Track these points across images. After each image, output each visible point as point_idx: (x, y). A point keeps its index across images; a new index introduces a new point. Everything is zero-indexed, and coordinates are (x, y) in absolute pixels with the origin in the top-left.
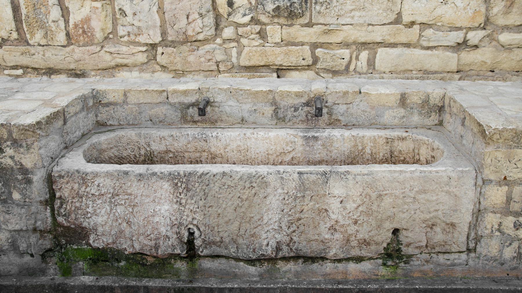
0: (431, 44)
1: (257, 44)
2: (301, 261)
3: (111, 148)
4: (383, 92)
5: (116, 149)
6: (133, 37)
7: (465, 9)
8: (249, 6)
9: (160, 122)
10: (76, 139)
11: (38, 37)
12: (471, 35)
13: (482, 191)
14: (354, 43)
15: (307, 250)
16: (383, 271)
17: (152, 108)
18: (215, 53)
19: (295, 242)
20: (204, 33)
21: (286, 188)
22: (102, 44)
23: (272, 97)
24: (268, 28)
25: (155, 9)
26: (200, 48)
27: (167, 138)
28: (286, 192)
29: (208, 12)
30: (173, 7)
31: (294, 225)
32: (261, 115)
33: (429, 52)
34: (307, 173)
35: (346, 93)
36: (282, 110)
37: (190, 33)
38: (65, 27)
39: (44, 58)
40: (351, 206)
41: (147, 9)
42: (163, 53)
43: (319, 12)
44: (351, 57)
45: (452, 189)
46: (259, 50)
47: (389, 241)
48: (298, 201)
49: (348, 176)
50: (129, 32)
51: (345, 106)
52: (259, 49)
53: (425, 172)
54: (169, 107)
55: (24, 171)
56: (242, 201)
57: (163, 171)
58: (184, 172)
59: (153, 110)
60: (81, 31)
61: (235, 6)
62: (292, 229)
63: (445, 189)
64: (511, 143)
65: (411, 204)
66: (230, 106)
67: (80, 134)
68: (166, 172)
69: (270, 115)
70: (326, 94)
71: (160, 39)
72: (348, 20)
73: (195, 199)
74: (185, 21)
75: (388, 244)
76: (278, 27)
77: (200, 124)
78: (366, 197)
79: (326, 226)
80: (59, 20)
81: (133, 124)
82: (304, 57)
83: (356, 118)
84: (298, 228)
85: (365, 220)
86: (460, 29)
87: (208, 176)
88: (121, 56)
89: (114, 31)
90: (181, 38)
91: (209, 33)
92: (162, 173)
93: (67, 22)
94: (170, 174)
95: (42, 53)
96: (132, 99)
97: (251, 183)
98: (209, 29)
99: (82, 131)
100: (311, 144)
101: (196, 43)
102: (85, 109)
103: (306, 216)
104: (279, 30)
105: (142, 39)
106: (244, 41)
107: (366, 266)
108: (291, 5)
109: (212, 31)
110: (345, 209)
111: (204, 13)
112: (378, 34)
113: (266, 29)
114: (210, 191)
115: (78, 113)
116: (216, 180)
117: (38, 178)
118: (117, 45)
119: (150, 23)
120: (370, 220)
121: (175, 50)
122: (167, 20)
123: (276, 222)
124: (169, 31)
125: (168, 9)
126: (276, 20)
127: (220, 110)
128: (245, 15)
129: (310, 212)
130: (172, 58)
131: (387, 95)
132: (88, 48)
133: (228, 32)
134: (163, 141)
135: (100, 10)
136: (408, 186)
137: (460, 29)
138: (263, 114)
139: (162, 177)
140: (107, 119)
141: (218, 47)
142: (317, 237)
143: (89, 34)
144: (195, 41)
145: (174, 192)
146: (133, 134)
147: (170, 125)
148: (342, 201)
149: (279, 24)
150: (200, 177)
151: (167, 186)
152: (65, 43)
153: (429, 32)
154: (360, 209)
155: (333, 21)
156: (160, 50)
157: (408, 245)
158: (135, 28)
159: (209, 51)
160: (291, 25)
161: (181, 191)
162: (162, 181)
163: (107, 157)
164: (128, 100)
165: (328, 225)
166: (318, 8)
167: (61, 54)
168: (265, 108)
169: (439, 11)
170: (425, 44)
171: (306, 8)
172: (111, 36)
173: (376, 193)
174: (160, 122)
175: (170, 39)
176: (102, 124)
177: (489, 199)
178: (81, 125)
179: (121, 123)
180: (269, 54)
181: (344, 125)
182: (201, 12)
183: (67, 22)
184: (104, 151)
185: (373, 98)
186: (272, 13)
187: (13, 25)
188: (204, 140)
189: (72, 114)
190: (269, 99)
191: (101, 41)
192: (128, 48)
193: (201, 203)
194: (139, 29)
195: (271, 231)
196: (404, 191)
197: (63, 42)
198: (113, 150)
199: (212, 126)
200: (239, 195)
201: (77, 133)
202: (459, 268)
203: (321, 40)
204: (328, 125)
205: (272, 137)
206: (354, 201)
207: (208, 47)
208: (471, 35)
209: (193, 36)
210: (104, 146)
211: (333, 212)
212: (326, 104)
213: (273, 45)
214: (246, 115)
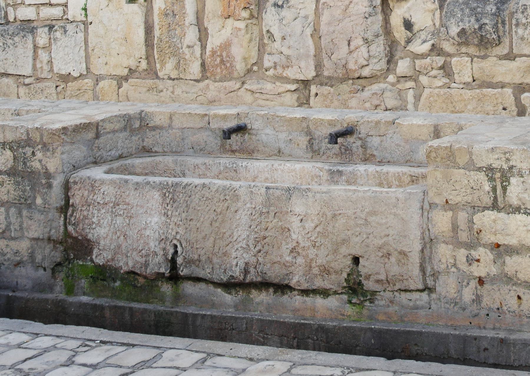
1: (440, 84)
2: (271, 290)
4: (415, 123)
6: (280, 70)
8: (432, 29)
9: (201, 150)
11: (168, 68)
13: (430, 216)
15: (274, 274)
16: (349, 310)
17: (195, 134)
18: (384, 96)
19: (260, 264)
20: (370, 67)
21: (254, 203)
22: (243, 79)
23: (306, 125)
24: (454, 60)
25: (309, 31)
26: (366, 89)
27: (200, 166)
28: (254, 207)
29: (377, 36)
30: (332, 29)
31: (259, 244)
32: (296, 146)
34: (274, 189)
35: (378, 123)
36: (317, 141)
37: (352, 66)
38: (201, 54)
39: (173, 96)
40: (309, 225)
41: (299, 32)
42: (317, 94)
43: (522, 39)
45: (399, 211)
46: (442, 93)
47: (348, 270)
48: (263, 217)
49: (309, 194)
50: (275, 63)
51: (378, 138)
52: (442, 91)
53: (376, 192)
54: (210, 133)
56: (217, 215)
57: (155, 180)
58: (173, 181)
59: (195, 137)
60: (218, 60)
61: (416, 28)
62: (257, 248)
63: (393, 211)
64: (449, 162)
65: (363, 227)
66: (265, 134)
68: (158, 182)
69: (304, 147)
70: (359, 123)
71: (314, 74)
73: (179, 211)
74: (345, 49)
75: (349, 275)
76: (467, 59)
77: (237, 154)
78: (322, 217)
79: (288, 247)
80: (195, 44)
81: (176, 152)
82: (505, 106)
83: (391, 153)
84: (263, 247)
85: (322, 242)
87: (190, 187)
88: (264, 97)
89: (259, 62)
90: (340, 72)
91: (378, 67)
92: (154, 182)
93: (203, 47)
94: (161, 183)
95: (171, 89)
96: (177, 123)
97: (225, 195)
98: (376, 60)
100: (335, 179)
101: (360, 81)
102: (128, 130)
103: (270, 234)
104: (469, 64)
105: (291, 73)
106: (424, 80)
107: (333, 302)
108: (480, 28)
109: (383, 64)
110: (304, 229)
111: (370, 38)
113: (451, 62)
114: (191, 202)
116: (196, 191)
118: (261, 81)
119: (301, 51)
120: (326, 243)
121: (332, 90)
122: (323, 47)
123: (244, 239)
124: (326, 62)
125: (325, 32)
126: (464, 49)
127: (257, 138)
128: (424, 42)
129: (274, 229)
130: (329, 101)
131: (419, 126)
132: (225, 84)
133: (403, 66)
134: (197, 170)
135: (243, 32)
136: (360, 206)
138: (298, 145)
139: (153, 186)
140: (152, 144)
141: (390, 87)
142: (279, 259)
143: (228, 65)
144: (359, 78)
145: (163, 203)
146: (171, 161)
148: (302, 220)
149: (468, 55)
150: (184, 188)
151: (157, 195)
152: (198, 76)
154: (318, 229)
156: (314, 89)
157: (368, 277)
158: (283, 58)
159: (376, 93)
161: (168, 202)
162: (154, 190)
164: (173, 124)
165: (290, 246)
166: (520, 31)
167: (193, 91)
168: (300, 138)
171: (504, 32)
172: (255, 68)
173: (331, 212)
174: (201, 150)
175: (326, 73)
176: (148, 150)
177: (437, 226)
179: (165, 150)
180: (456, 100)
181: (379, 162)
182: (366, 36)
183: (203, 47)
185: (405, 129)
186: (457, 38)
188: (235, 171)
190: (303, 128)
191: (242, 75)
192: (274, 85)
193: (184, 215)
194: (288, 59)
195: (240, 249)
196: (356, 211)
197: (196, 75)
199: (249, 157)
200: (214, 208)
202: (422, 312)
204: (363, 161)
205: (298, 169)
206: (312, 220)
207: (376, 87)
209: (356, 70)
211: (294, 232)
212: (359, 136)
213: (461, 86)
214: (282, 146)
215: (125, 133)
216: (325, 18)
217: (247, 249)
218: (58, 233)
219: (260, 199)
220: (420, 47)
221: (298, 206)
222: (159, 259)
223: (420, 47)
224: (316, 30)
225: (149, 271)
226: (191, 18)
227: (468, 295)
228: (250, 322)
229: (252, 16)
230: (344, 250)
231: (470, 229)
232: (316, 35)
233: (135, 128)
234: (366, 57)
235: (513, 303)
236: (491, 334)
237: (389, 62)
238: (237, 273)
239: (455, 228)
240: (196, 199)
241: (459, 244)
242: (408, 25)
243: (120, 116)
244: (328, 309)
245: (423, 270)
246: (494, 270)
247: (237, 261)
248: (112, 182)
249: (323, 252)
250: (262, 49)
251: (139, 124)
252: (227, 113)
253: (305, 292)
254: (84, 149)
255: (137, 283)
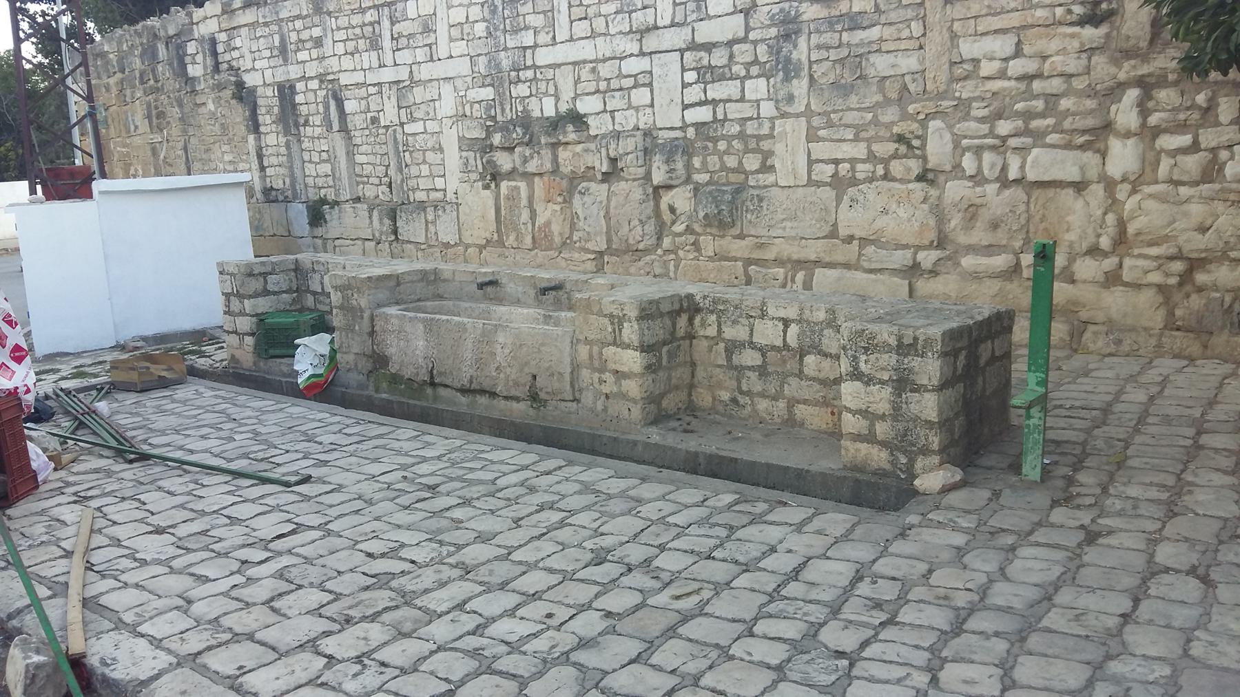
0: (873, 266)
7: (909, 220)
11: (511, 240)
12: (921, 256)
14: (789, 260)
15: (487, 385)
16: (532, 412)
25: (602, 213)
29: (649, 218)
33: (873, 276)
37: (631, 241)
40: (507, 351)
44: (786, 278)
55: (362, 311)
61: (678, 212)
66: (511, 288)
72: (779, 232)
86: (906, 247)
90: (623, 246)
91: (649, 243)
93: (533, 225)
96: (457, 278)
105: (590, 246)
106: (681, 253)
108: (719, 213)
109: (653, 241)
112: (812, 251)
117: (366, 315)
124: (614, 238)
126: (708, 230)
133: (667, 242)
137: (906, 247)
147: (477, 300)
149: (711, 234)
153: (870, 250)
155: (764, 232)
157: (541, 390)
160: (723, 236)
169: (880, 223)
170: (866, 265)
183: (533, 225)
187: (493, 227)
202: (573, 416)
203: (755, 256)
208: (921, 256)
216: (613, 204)
217: (471, 366)
218: (368, 351)
219: (479, 332)
220: (679, 228)
221: (501, 338)
222: (424, 371)
223: (679, 228)
224: (607, 212)
225: (419, 378)
226: (524, 202)
227: (600, 407)
228: (472, 416)
229: (565, 201)
230: (526, 370)
231: (601, 358)
232: (607, 216)
234: (639, 234)
235: (627, 412)
236: (608, 434)
237: (658, 239)
238: (466, 382)
239: (591, 357)
240: (443, 329)
241: (594, 370)
242: (672, 210)
244: (520, 410)
245: (572, 386)
246: (615, 389)
247: (465, 374)
248: (397, 316)
249: (514, 371)
250: (573, 227)
252: (547, 276)
253: (506, 398)
254: (387, 293)
255: (414, 387)
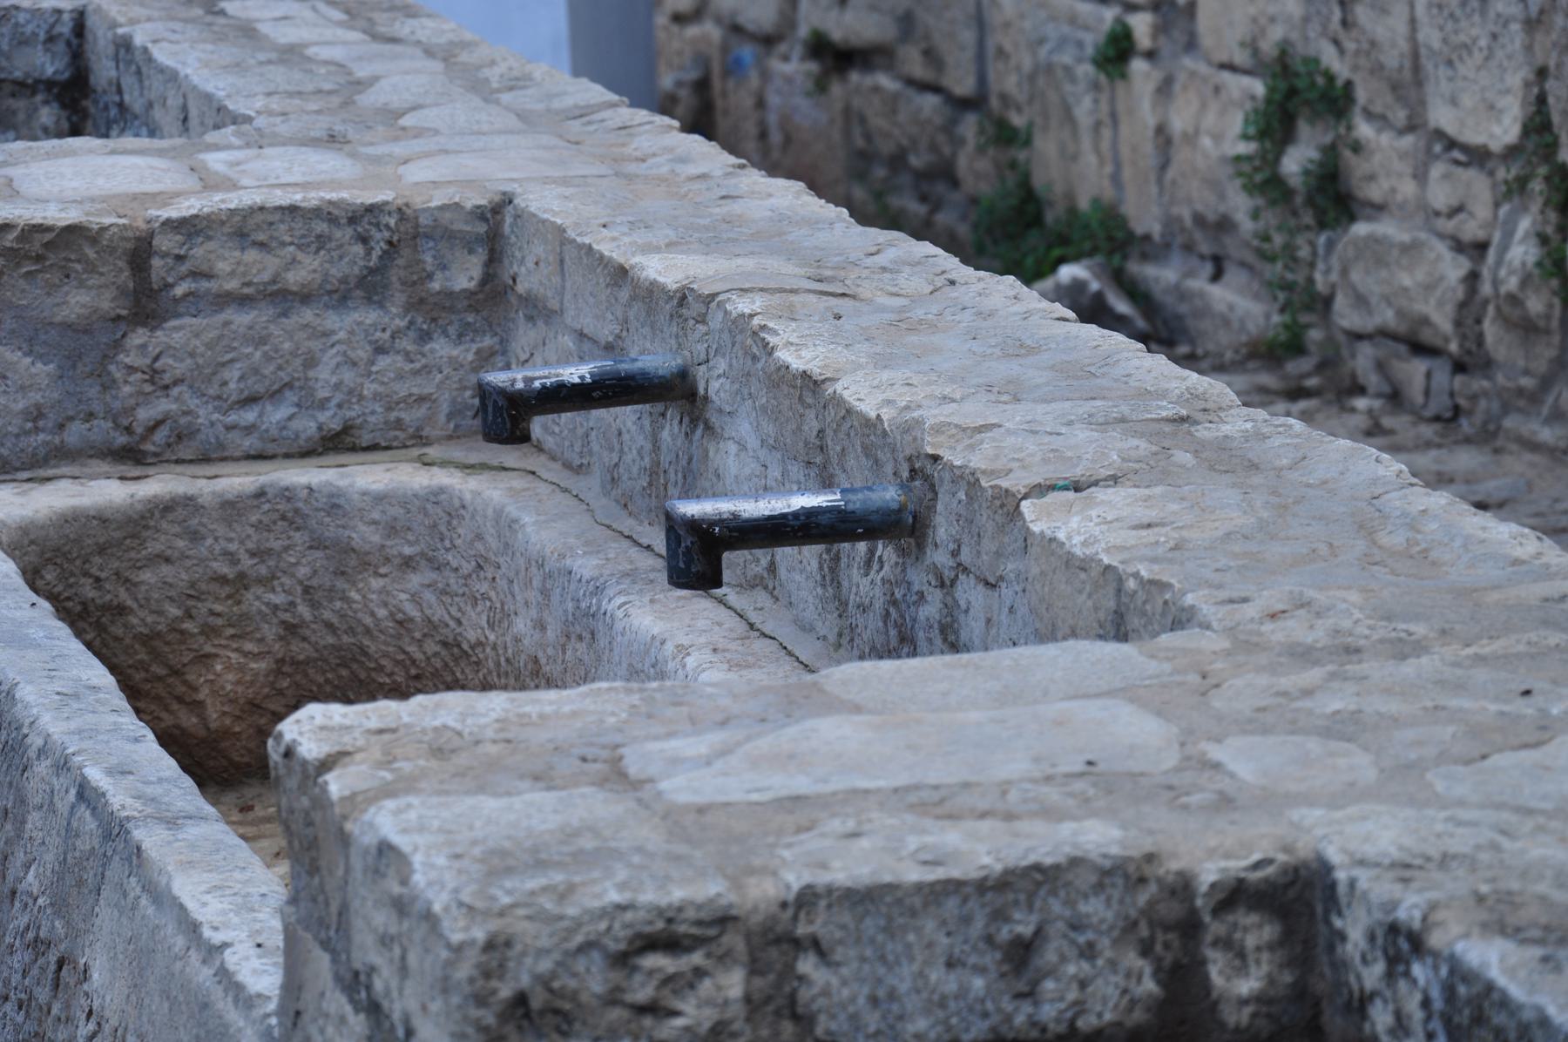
3: (408, 563)
5: (431, 576)
10: (249, 443)
67: (307, 427)
99: (330, 419)
115: (305, 297)
163: (382, 613)
178: (324, 374)
184: (367, 563)
189: (232, 285)
198: (415, 580)
201: (276, 414)
210: (365, 536)
215: (371, 316)
233: (450, 294)
243: (326, 214)
251: (477, 272)
